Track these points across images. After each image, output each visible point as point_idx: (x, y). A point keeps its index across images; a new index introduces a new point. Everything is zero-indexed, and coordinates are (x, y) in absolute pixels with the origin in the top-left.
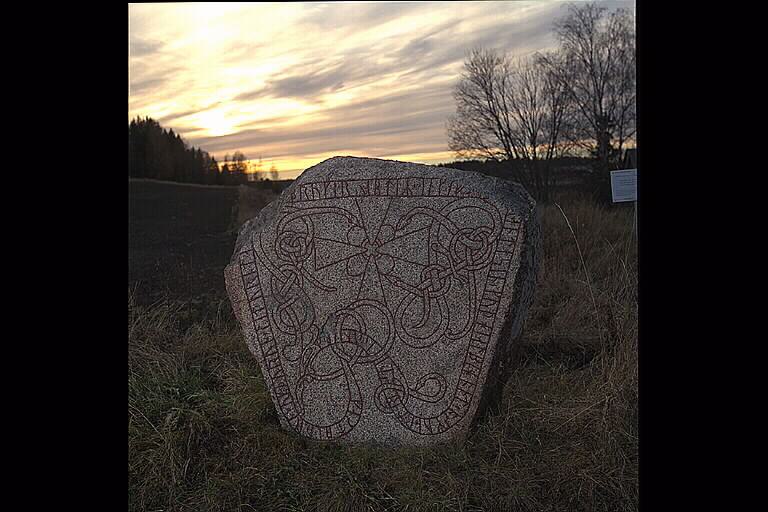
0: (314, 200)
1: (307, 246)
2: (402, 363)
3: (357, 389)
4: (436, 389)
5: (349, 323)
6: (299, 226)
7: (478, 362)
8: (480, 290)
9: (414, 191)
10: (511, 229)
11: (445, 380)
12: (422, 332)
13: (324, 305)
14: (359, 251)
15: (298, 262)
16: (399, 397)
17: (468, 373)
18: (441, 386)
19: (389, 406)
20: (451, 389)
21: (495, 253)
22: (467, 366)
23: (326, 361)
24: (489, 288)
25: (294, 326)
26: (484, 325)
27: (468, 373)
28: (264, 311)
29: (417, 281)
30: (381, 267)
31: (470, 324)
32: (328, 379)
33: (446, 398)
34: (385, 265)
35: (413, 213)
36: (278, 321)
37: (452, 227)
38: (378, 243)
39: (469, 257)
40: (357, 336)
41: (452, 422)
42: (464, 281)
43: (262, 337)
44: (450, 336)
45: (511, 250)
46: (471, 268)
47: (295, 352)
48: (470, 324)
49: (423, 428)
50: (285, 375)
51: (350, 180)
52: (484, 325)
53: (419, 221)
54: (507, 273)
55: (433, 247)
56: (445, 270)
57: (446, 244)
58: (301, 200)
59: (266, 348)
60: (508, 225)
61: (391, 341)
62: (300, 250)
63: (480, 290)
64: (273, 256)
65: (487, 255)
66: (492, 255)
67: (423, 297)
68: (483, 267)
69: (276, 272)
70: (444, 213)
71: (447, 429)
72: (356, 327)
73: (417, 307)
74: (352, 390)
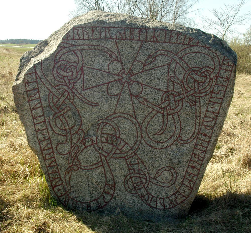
0: (84, 39)
1: (77, 73)
2: (145, 159)
3: (111, 176)
4: (169, 178)
5: (108, 129)
6: (73, 58)
7: (200, 160)
8: (204, 110)
9: (159, 39)
10: (227, 70)
11: (176, 172)
12: (161, 138)
13: (89, 116)
14: (117, 78)
15: (70, 83)
16: (142, 183)
17: (193, 167)
18: (173, 176)
19: (135, 189)
20: (179, 179)
21: (214, 86)
22: (192, 162)
23: (88, 156)
24: (210, 109)
25: (65, 130)
26: (205, 135)
27: (193, 167)
28: (43, 117)
29: (159, 102)
30: (133, 91)
31: (195, 134)
32: (91, 169)
33: (176, 184)
34: (136, 88)
35: (158, 53)
36: (53, 124)
37: (185, 65)
38: (131, 73)
39: (196, 88)
40: (113, 139)
41: (179, 200)
42: (193, 104)
43: (40, 137)
44: (180, 140)
45: (225, 84)
46: (198, 95)
47: (66, 148)
48: (195, 134)
49: (159, 205)
50: (57, 165)
51: (111, 27)
52: (205, 135)
53: (160, 61)
54: (222, 99)
55: (171, 80)
56: (179, 95)
57: (181, 77)
58: (74, 39)
59: (43, 144)
60: (224, 67)
61: (138, 143)
62: (72, 76)
63: (204, 110)
64: (50, 77)
65: (209, 87)
66: (212, 87)
67: (163, 113)
68: (206, 95)
69: (53, 90)
70: (180, 55)
71: (176, 206)
72: (112, 132)
73: (157, 122)
74: (108, 177)
